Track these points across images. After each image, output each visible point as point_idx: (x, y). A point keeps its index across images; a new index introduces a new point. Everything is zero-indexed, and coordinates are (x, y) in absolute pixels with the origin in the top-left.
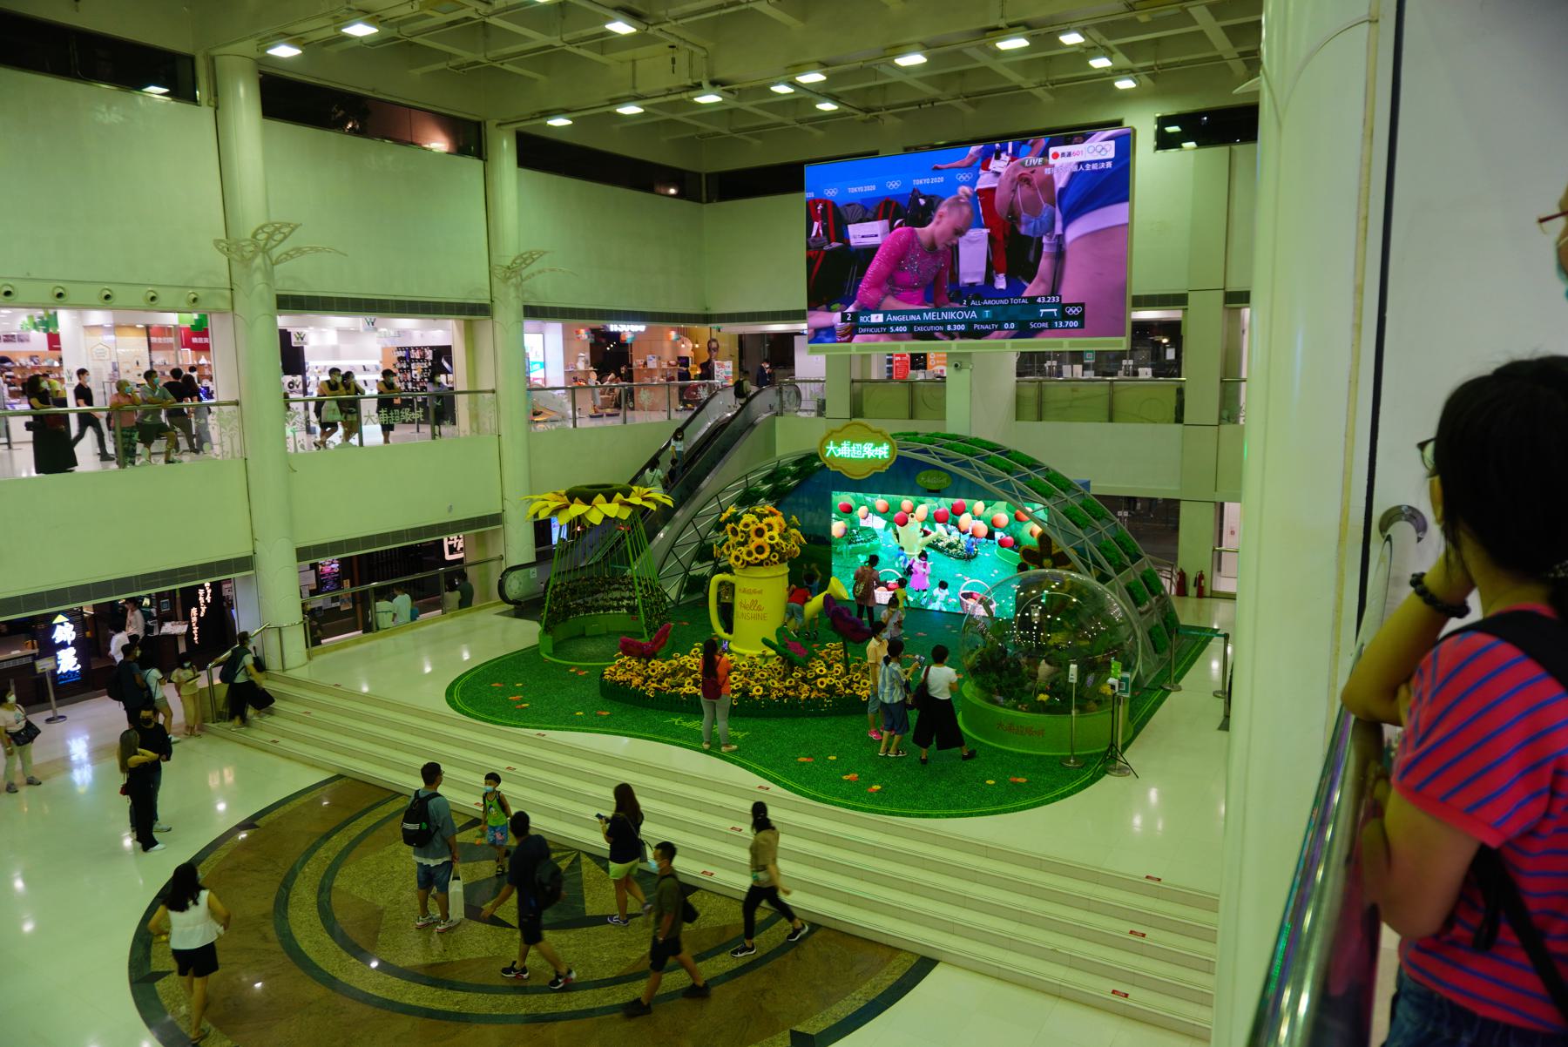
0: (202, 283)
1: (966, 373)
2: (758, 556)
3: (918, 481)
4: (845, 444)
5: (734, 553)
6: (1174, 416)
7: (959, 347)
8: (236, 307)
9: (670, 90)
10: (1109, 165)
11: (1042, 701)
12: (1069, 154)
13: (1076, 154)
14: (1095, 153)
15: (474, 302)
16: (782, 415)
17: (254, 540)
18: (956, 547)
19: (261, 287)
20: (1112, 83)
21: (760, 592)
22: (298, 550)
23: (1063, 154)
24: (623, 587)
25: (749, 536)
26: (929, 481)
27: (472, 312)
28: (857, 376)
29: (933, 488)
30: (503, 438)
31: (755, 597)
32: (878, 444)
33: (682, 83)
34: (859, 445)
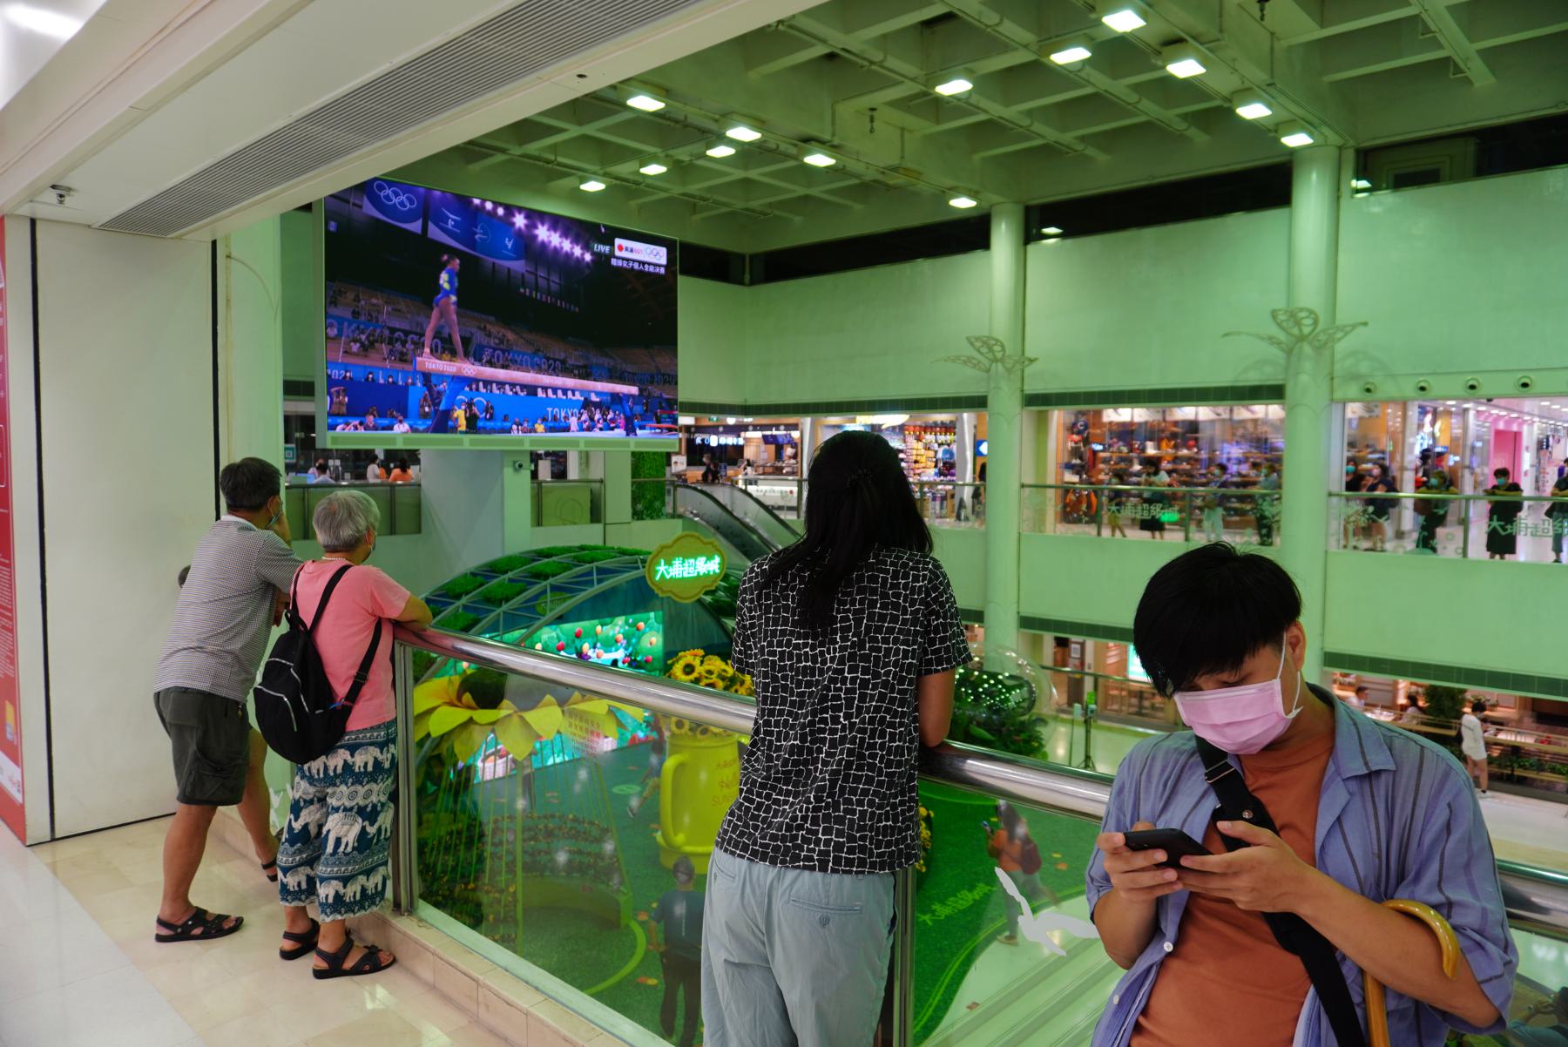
4: (677, 562)
13: (638, 252)
23: (627, 249)
34: (692, 561)
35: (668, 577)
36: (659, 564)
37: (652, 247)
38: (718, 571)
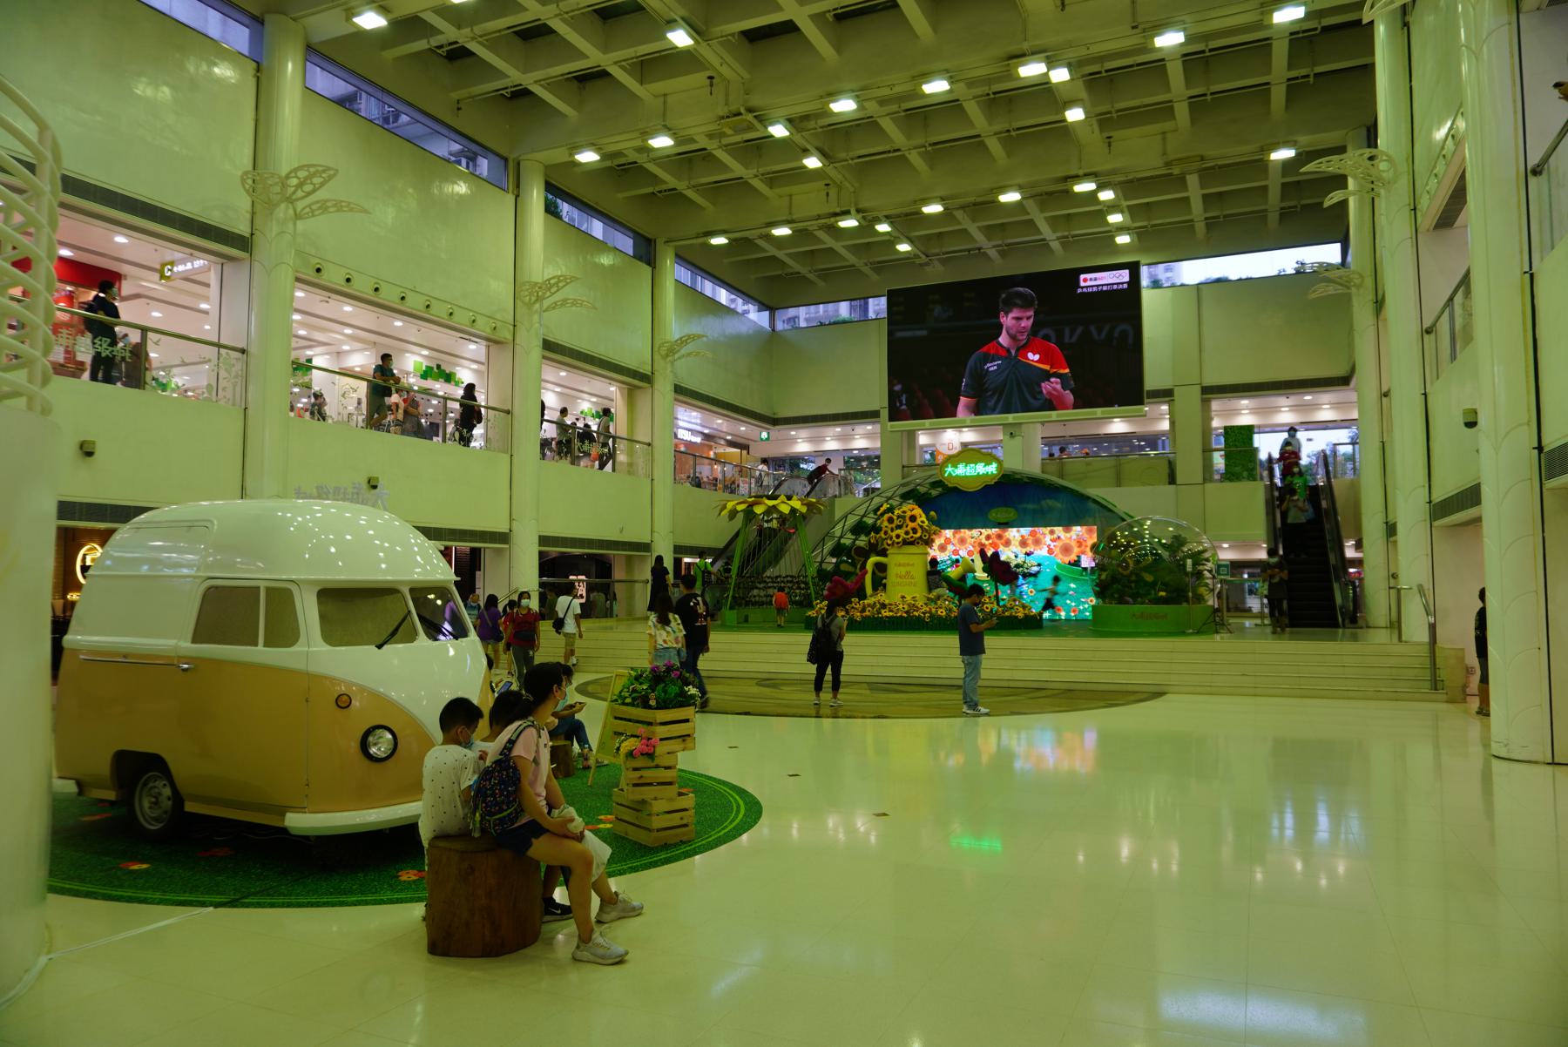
0: (498, 316)
1: (1018, 439)
2: (915, 536)
3: (990, 517)
5: (894, 534)
6: (1167, 481)
7: (1014, 418)
8: (517, 341)
9: (819, 216)
10: (1125, 286)
11: (1162, 596)
12: (1096, 279)
13: (1101, 279)
14: (1115, 278)
15: (641, 371)
16: (840, 496)
17: (511, 520)
18: (1022, 566)
19: (537, 325)
20: (1113, 238)
21: (913, 565)
22: (540, 536)
23: (1091, 279)
24: (775, 585)
25: (905, 520)
26: (999, 516)
27: (637, 380)
28: (905, 463)
29: (1002, 521)
30: (655, 482)
31: (908, 569)
32: (988, 464)
33: (832, 211)
35: (954, 475)
36: (947, 467)
37: (1114, 272)
38: (995, 472)
